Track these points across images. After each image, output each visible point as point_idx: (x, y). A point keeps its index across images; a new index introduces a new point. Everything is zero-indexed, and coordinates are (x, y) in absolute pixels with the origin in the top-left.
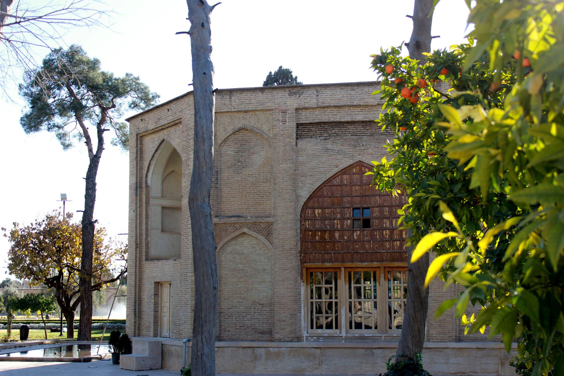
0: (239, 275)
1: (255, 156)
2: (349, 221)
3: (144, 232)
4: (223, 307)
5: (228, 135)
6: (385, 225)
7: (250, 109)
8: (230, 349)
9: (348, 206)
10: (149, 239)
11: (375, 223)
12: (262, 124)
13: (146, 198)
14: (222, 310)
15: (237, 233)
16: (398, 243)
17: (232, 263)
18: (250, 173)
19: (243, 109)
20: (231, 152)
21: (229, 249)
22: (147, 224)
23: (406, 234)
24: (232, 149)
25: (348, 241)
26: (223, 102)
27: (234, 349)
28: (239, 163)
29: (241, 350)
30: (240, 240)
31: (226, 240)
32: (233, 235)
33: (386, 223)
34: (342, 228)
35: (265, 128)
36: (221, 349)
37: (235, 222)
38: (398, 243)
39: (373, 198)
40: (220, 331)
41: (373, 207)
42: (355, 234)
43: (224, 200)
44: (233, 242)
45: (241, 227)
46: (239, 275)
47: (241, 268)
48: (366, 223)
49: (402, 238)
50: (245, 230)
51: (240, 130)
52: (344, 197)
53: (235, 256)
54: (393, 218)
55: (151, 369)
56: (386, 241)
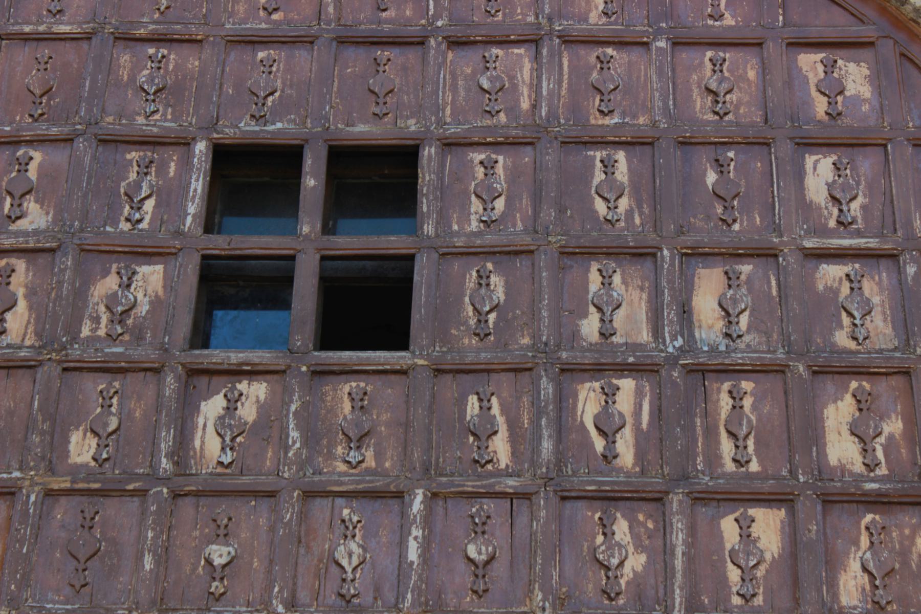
2: (151, 276)
6: (590, 327)
9: (162, 121)
11: (463, 303)
16: (768, 526)
23: (861, 434)
25: (98, 489)
33: (607, 309)
34: (46, 341)
38: (768, 526)
39: (465, 62)
41: (449, 145)
42: (213, 407)
48: (369, 310)
49: (822, 471)
52: (127, 39)
54: (696, 255)
56: (609, 499)
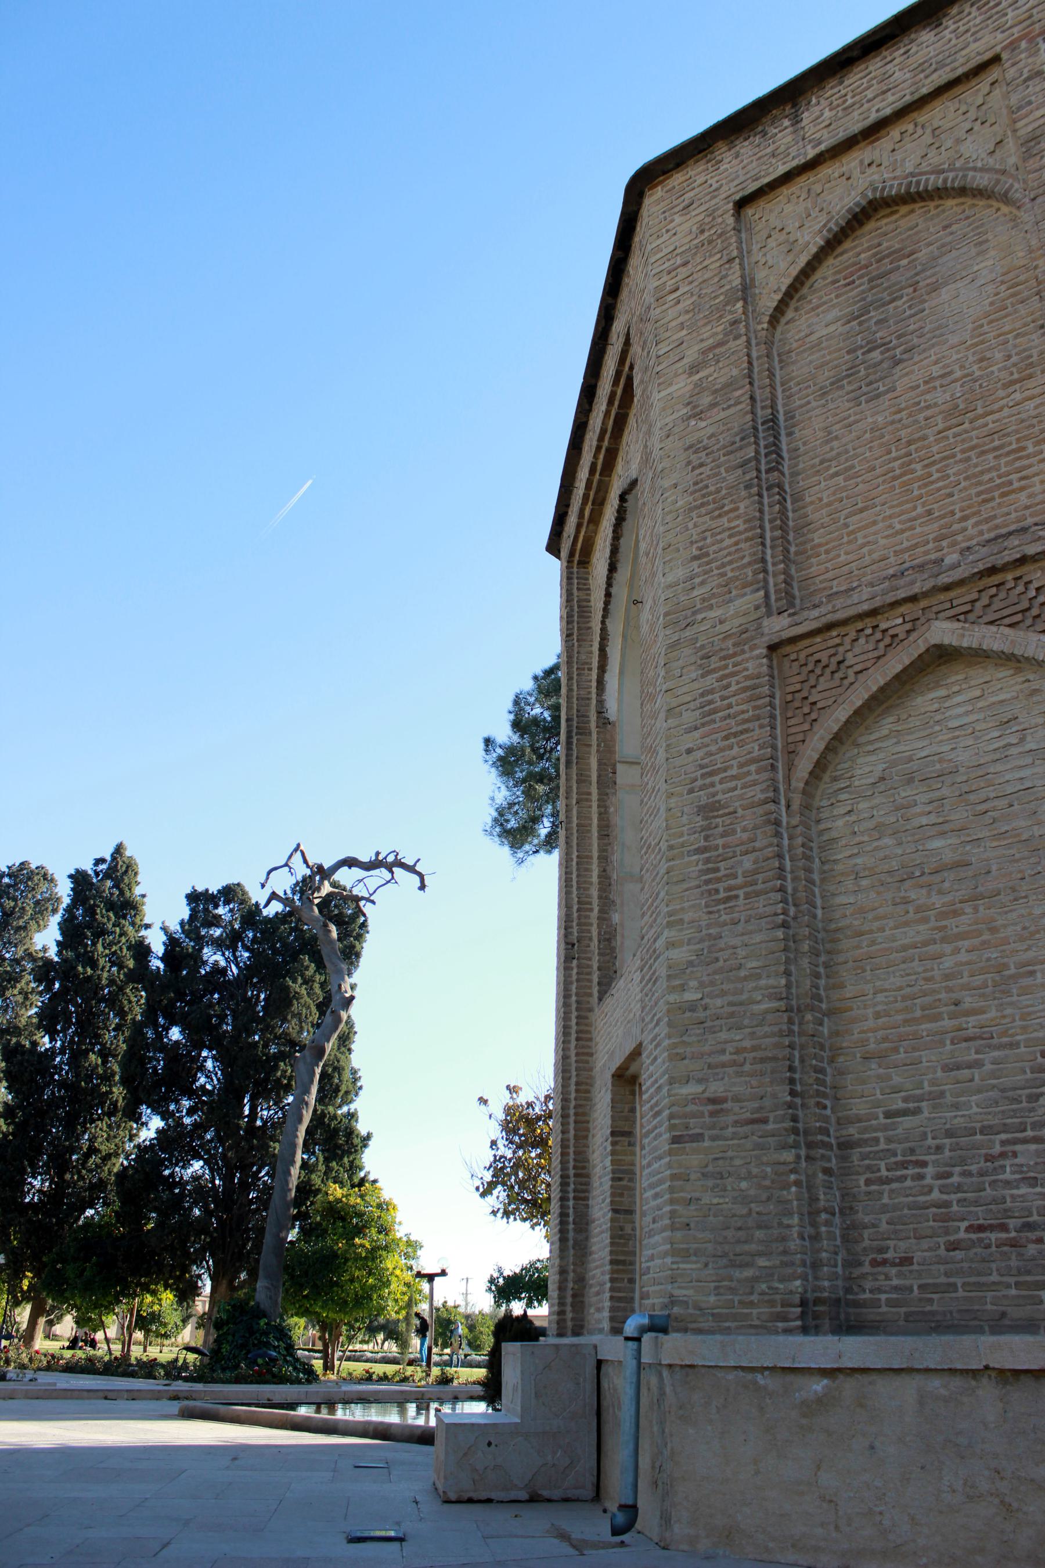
0: (938, 901)
1: (945, 294)
3: (594, 893)
4: (859, 1107)
5: (803, 260)
7: (888, 111)
8: (909, 1388)
10: (616, 918)
12: (958, 141)
13: (600, 763)
14: (852, 1131)
15: (896, 663)
17: (887, 841)
18: (936, 371)
19: (856, 128)
20: (832, 328)
21: (865, 765)
22: (604, 858)
24: (835, 313)
26: (769, 150)
27: (935, 1383)
28: (876, 355)
29: (987, 1390)
30: (924, 701)
31: (842, 713)
32: (877, 679)
35: (975, 149)
36: (849, 1386)
37: (877, 602)
40: (852, 1263)
43: (817, 538)
44: (887, 724)
45: (914, 625)
46: (938, 901)
47: (948, 857)
50: (943, 632)
51: (859, 218)
53: (905, 792)
55: (534, 1499)
